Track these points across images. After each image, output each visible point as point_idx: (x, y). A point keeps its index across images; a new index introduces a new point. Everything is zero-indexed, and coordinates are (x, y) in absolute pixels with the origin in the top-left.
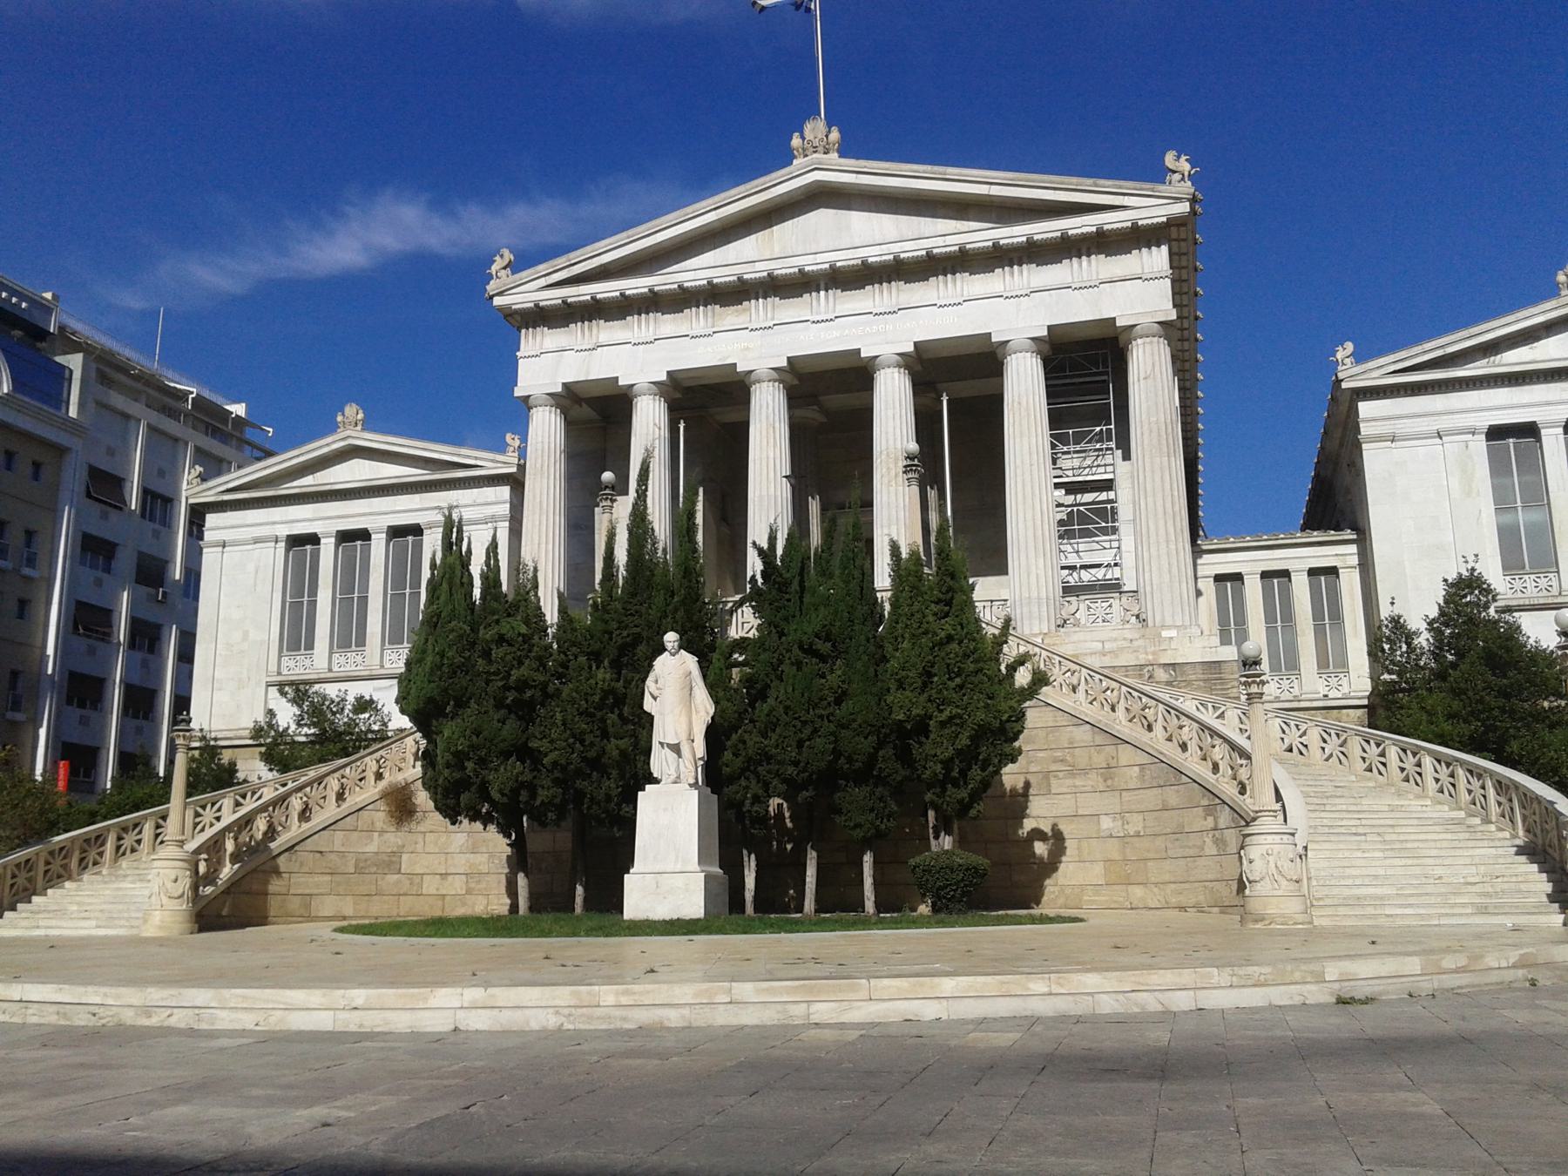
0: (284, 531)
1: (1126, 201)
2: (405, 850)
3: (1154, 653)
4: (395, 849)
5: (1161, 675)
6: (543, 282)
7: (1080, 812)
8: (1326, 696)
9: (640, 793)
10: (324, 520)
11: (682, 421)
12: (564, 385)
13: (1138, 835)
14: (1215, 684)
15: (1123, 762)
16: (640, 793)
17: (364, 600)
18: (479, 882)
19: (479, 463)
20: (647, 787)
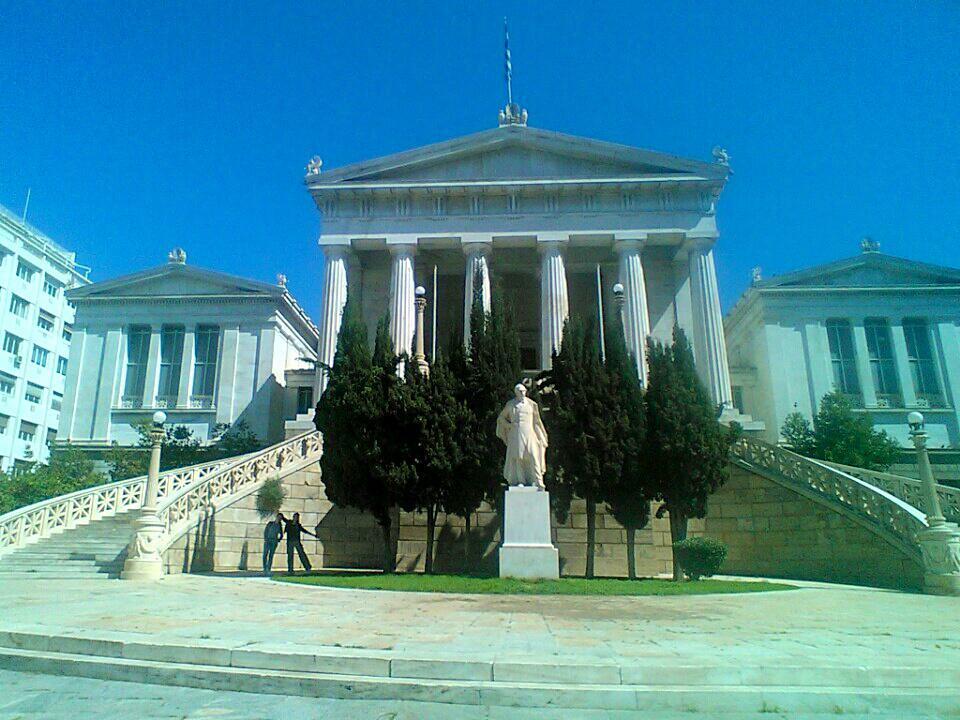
0: (127, 321)
10: (154, 318)
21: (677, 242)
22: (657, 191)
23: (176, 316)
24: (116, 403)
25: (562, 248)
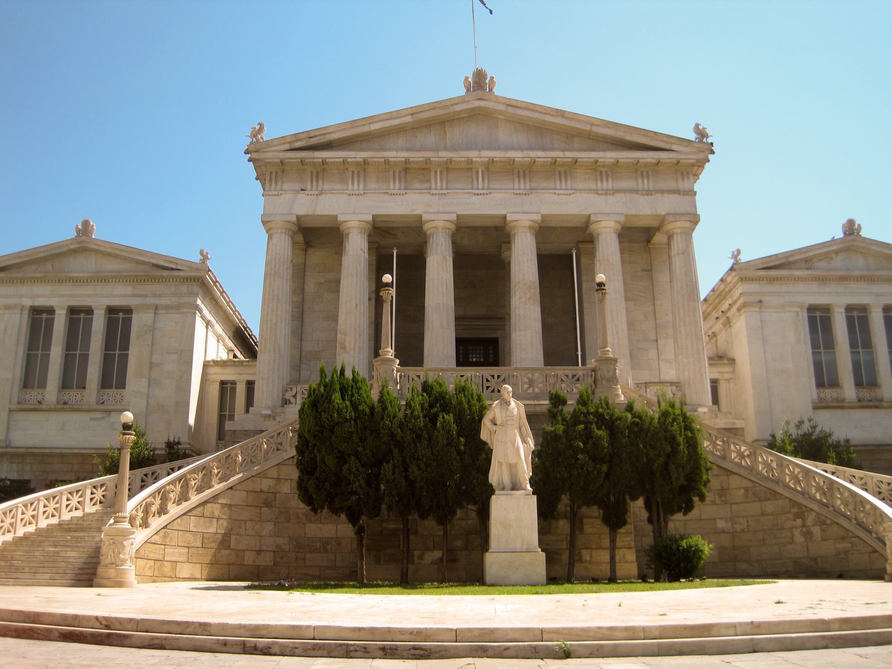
0: (28, 303)
1: (674, 147)
6: (288, 147)
7: (703, 517)
11: (395, 248)
12: (298, 217)
13: (743, 531)
17: (85, 358)
19: (179, 267)
21: (655, 224)
23: (83, 296)
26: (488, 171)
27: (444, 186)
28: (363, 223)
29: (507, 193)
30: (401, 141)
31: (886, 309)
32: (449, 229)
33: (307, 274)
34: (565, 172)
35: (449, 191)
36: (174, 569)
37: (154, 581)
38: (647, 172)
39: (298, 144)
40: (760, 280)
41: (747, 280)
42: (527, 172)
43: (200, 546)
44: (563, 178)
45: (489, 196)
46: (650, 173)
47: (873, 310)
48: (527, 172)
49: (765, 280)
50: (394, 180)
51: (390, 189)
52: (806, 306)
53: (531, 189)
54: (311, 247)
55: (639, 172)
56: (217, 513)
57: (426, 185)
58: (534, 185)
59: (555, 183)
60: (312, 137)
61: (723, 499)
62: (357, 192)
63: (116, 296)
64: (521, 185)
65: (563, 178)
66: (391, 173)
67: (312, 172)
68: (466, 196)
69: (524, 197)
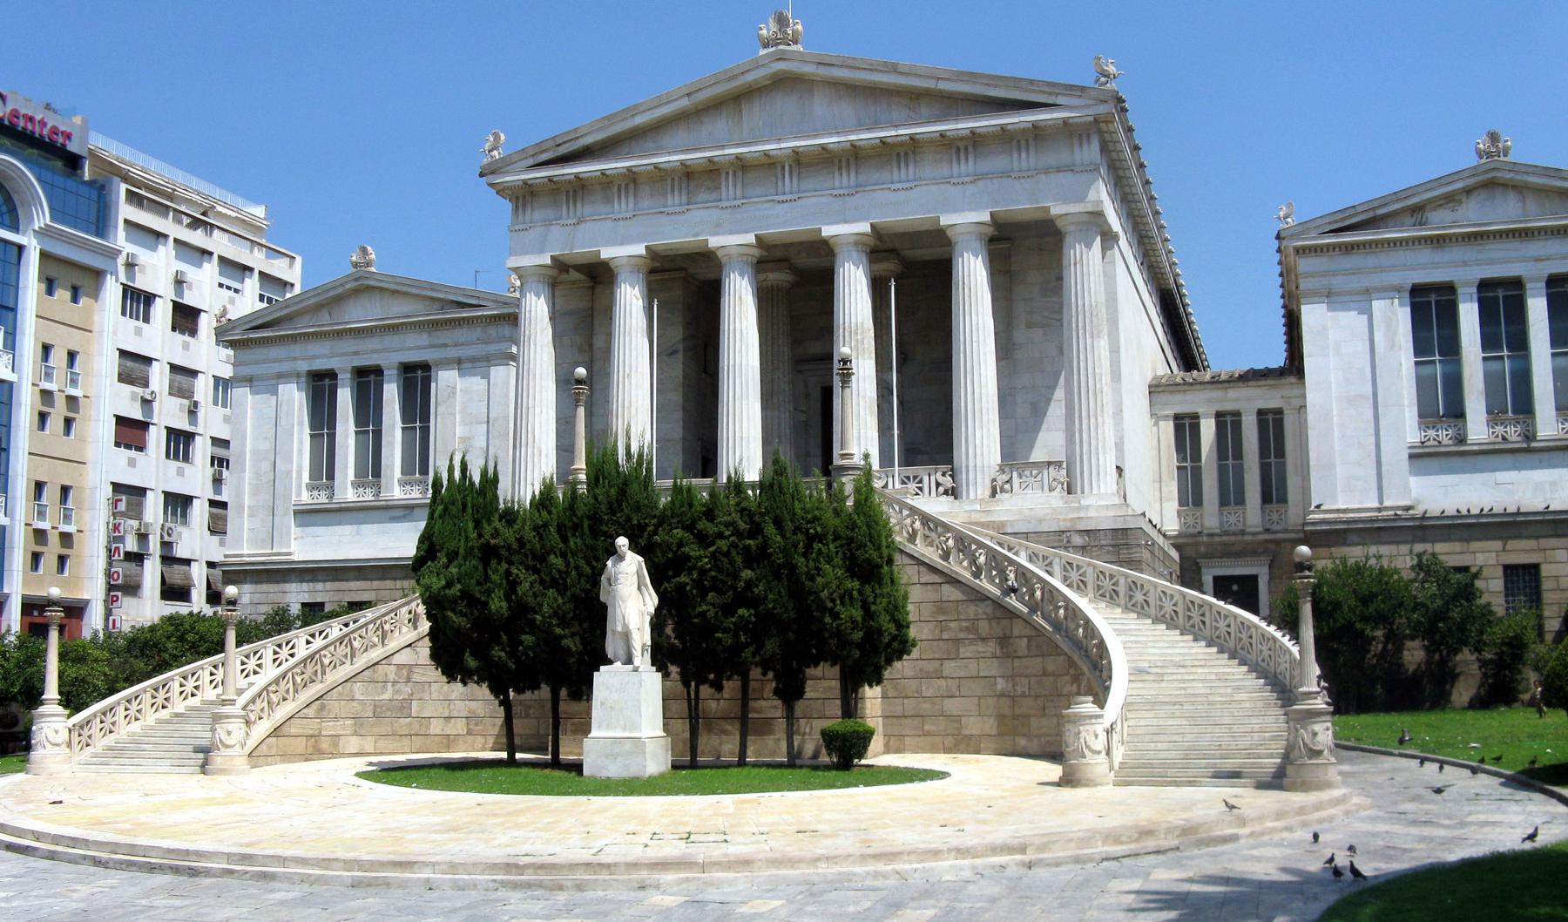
0: (304, 366)
1: (1060, 100)
2: (414, 697)
3: (1072, 520)
4: (406, 697)
5: (1078, 540)
6: (531, 162)
7: (981, 674)
8: (1268, 530)
9: (595, 673)
10: (341, 359)
13: (1023, 695)
14: (1122, 549)
15: (1016, 632)
16: (595, 673)
18: (477, 725)
19: (481, 303)
20: (602, 668)
22: (1005, 137)
23: (370, 353)
24: (299, 494)
25: (864, 244)
26: (799, 164)
27: (739, 193)
28: (556, 294)
29: (822, 196)
30: (681, 135)
31: (1553, 282)
32: (752, 256)
33: (596, 322)
34: (906, 154)
35: (744, 201)
36: (336, 745)
37: (307, 760)
38: (1027, 140)
39: (544, 157)
40: (1328, 251)
41: (1307, 252)
42: (852, 160)
43: (371, 715)
44: (902, 164)
45: (799, 203)
46: (1031, 142)
47: (1528, 286)
48: (852, 160)
49: (1337, 249)
50: (673, 191)
51: (666, 207)
52: (1409, 287)
53: (857, 186)
54: (600, 283)
55: (1014, 143)
56: (392, 677)
57: (714, 196)
58: (862, 178)
59: (892, 174)
60: (559, 145)
61: (1005, 650)
62: (624, 215)
63: (410, 349)
64: (844, 180)
65: (902, 164)
66: (669, 181)
67: (568, 192)
68: (766, 205)
69: (847, 198)
